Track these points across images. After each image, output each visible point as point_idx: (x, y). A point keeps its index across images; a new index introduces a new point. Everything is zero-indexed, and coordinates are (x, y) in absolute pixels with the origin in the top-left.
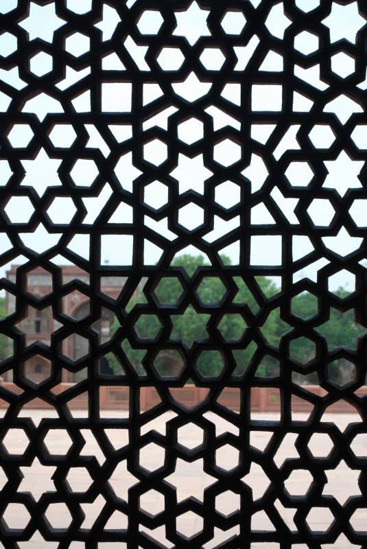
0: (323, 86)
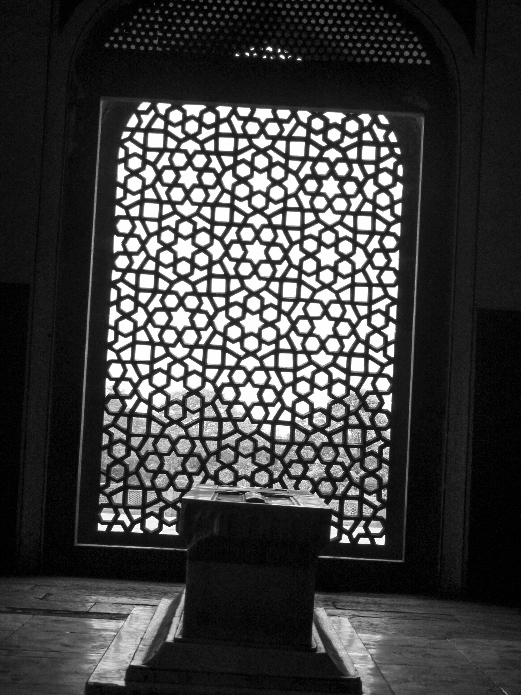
0: (324, 144)
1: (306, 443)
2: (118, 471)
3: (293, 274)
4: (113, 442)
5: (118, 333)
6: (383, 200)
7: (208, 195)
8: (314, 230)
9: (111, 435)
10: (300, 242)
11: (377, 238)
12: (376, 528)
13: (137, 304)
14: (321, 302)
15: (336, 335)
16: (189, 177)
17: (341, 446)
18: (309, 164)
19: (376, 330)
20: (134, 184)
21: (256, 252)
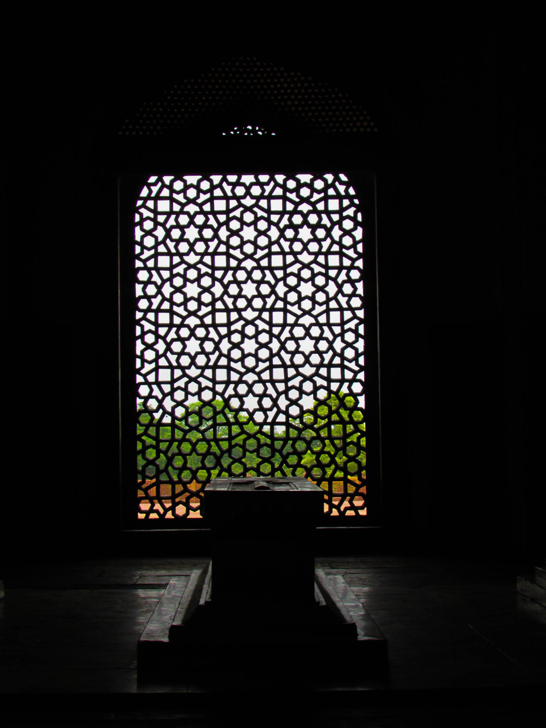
0: (297, 200)
1: (299, 438)
2: (151, 470)
3: (280, 304)
4: (145, 448)
5: (144, 361)
6: (347, 241)
7: (208, 247)
8: (294, 269)
9: (143, 442)
10: (284, 279)
11: (344, 272)
13: (158, 337)
14: (303, 326)
15: (317, 351)
16: (192, 233)
17: (326, 438)
18: (286, 216)
19: (349, 345)
20: (149, 241)
21: (249, 289)
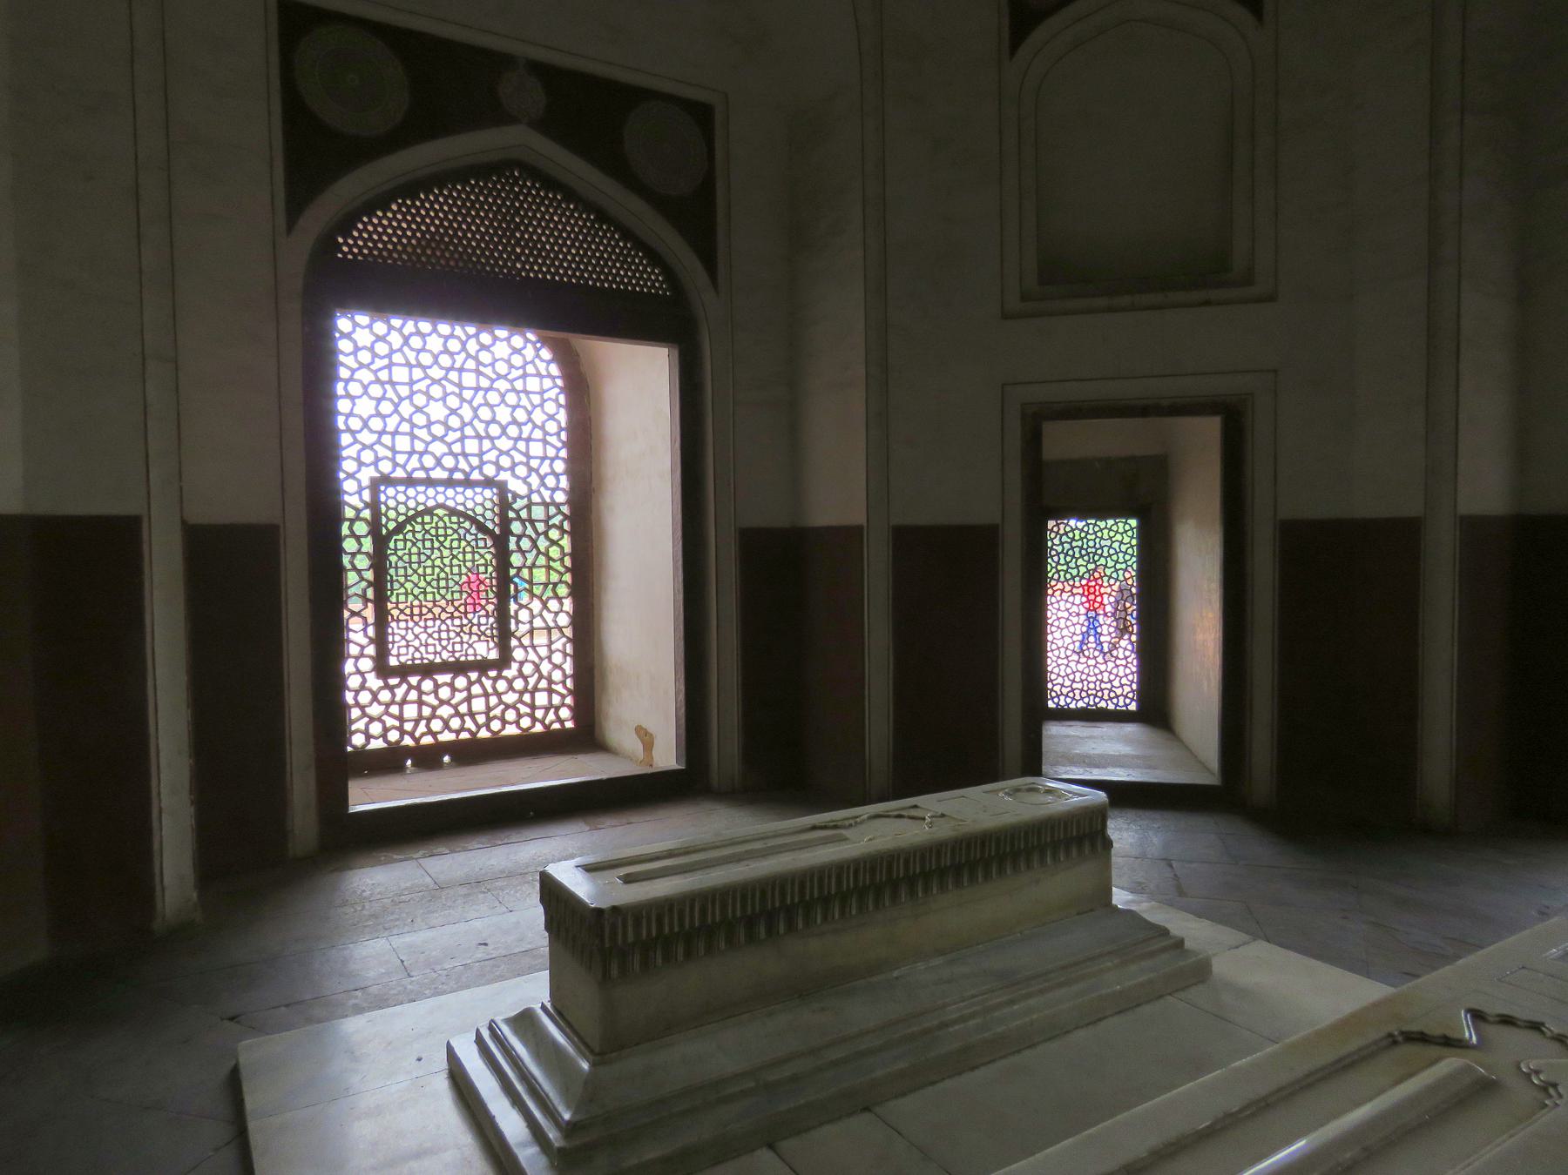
12: (565, 713)
19: (553, 543)
